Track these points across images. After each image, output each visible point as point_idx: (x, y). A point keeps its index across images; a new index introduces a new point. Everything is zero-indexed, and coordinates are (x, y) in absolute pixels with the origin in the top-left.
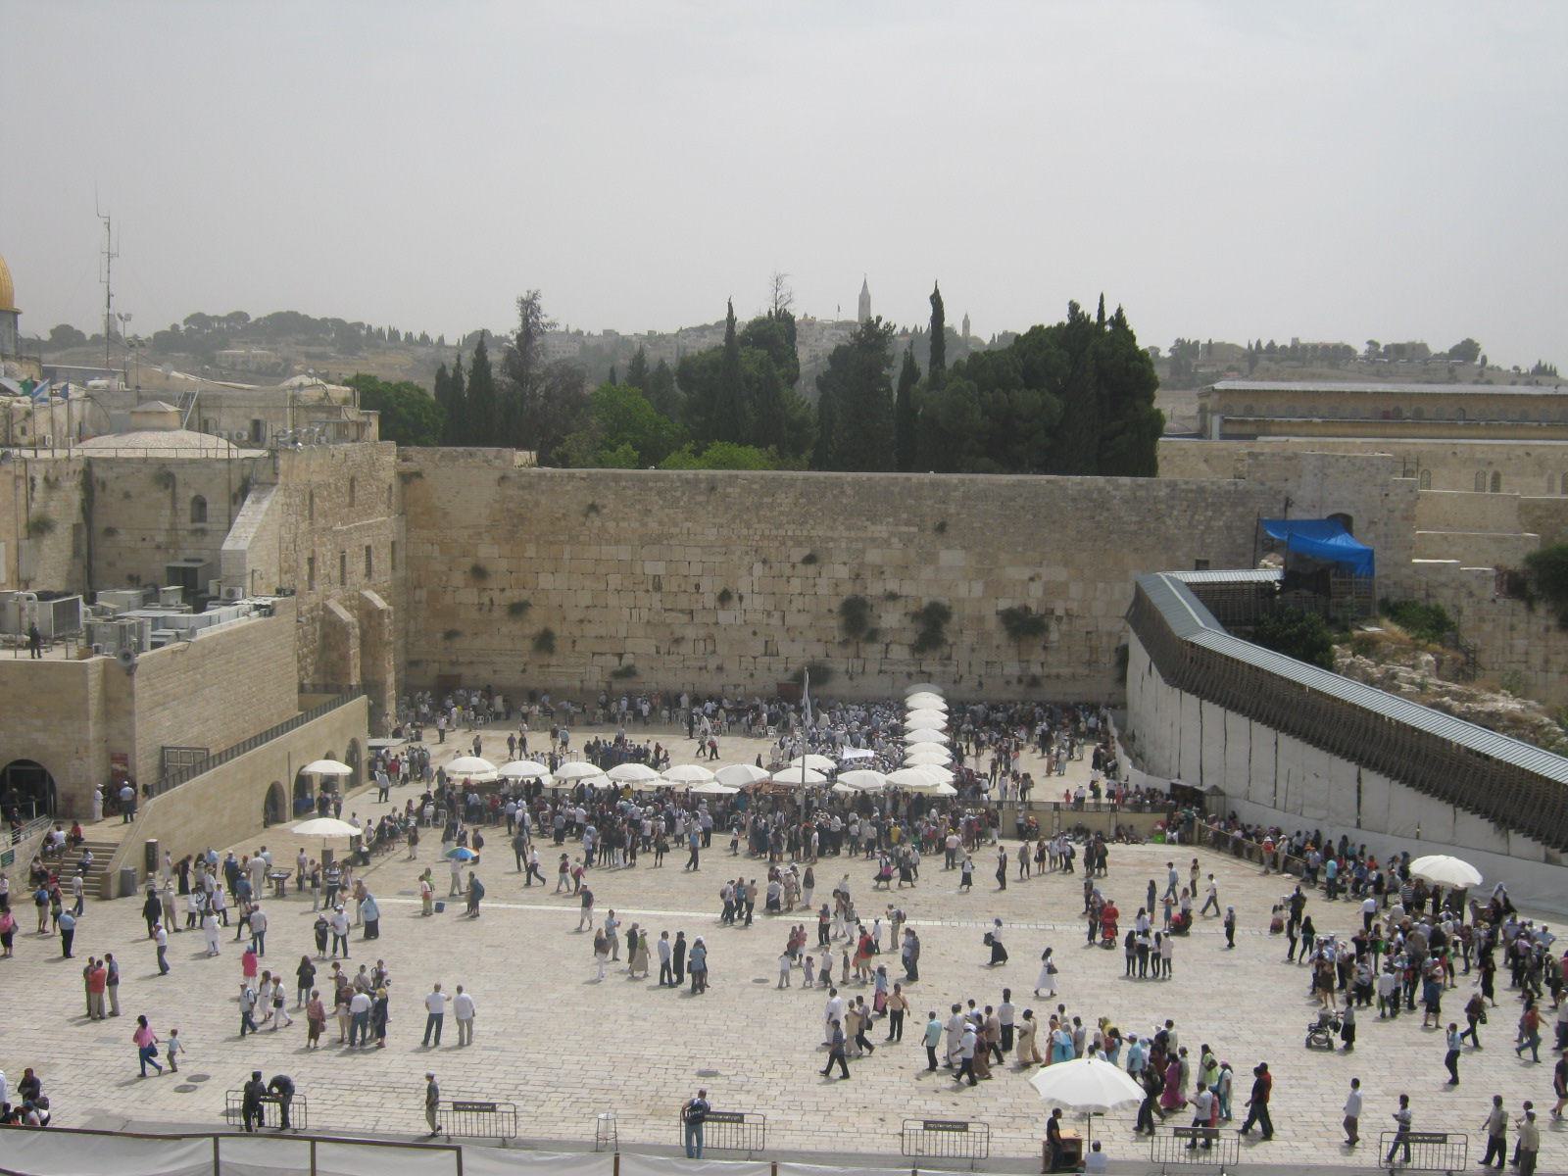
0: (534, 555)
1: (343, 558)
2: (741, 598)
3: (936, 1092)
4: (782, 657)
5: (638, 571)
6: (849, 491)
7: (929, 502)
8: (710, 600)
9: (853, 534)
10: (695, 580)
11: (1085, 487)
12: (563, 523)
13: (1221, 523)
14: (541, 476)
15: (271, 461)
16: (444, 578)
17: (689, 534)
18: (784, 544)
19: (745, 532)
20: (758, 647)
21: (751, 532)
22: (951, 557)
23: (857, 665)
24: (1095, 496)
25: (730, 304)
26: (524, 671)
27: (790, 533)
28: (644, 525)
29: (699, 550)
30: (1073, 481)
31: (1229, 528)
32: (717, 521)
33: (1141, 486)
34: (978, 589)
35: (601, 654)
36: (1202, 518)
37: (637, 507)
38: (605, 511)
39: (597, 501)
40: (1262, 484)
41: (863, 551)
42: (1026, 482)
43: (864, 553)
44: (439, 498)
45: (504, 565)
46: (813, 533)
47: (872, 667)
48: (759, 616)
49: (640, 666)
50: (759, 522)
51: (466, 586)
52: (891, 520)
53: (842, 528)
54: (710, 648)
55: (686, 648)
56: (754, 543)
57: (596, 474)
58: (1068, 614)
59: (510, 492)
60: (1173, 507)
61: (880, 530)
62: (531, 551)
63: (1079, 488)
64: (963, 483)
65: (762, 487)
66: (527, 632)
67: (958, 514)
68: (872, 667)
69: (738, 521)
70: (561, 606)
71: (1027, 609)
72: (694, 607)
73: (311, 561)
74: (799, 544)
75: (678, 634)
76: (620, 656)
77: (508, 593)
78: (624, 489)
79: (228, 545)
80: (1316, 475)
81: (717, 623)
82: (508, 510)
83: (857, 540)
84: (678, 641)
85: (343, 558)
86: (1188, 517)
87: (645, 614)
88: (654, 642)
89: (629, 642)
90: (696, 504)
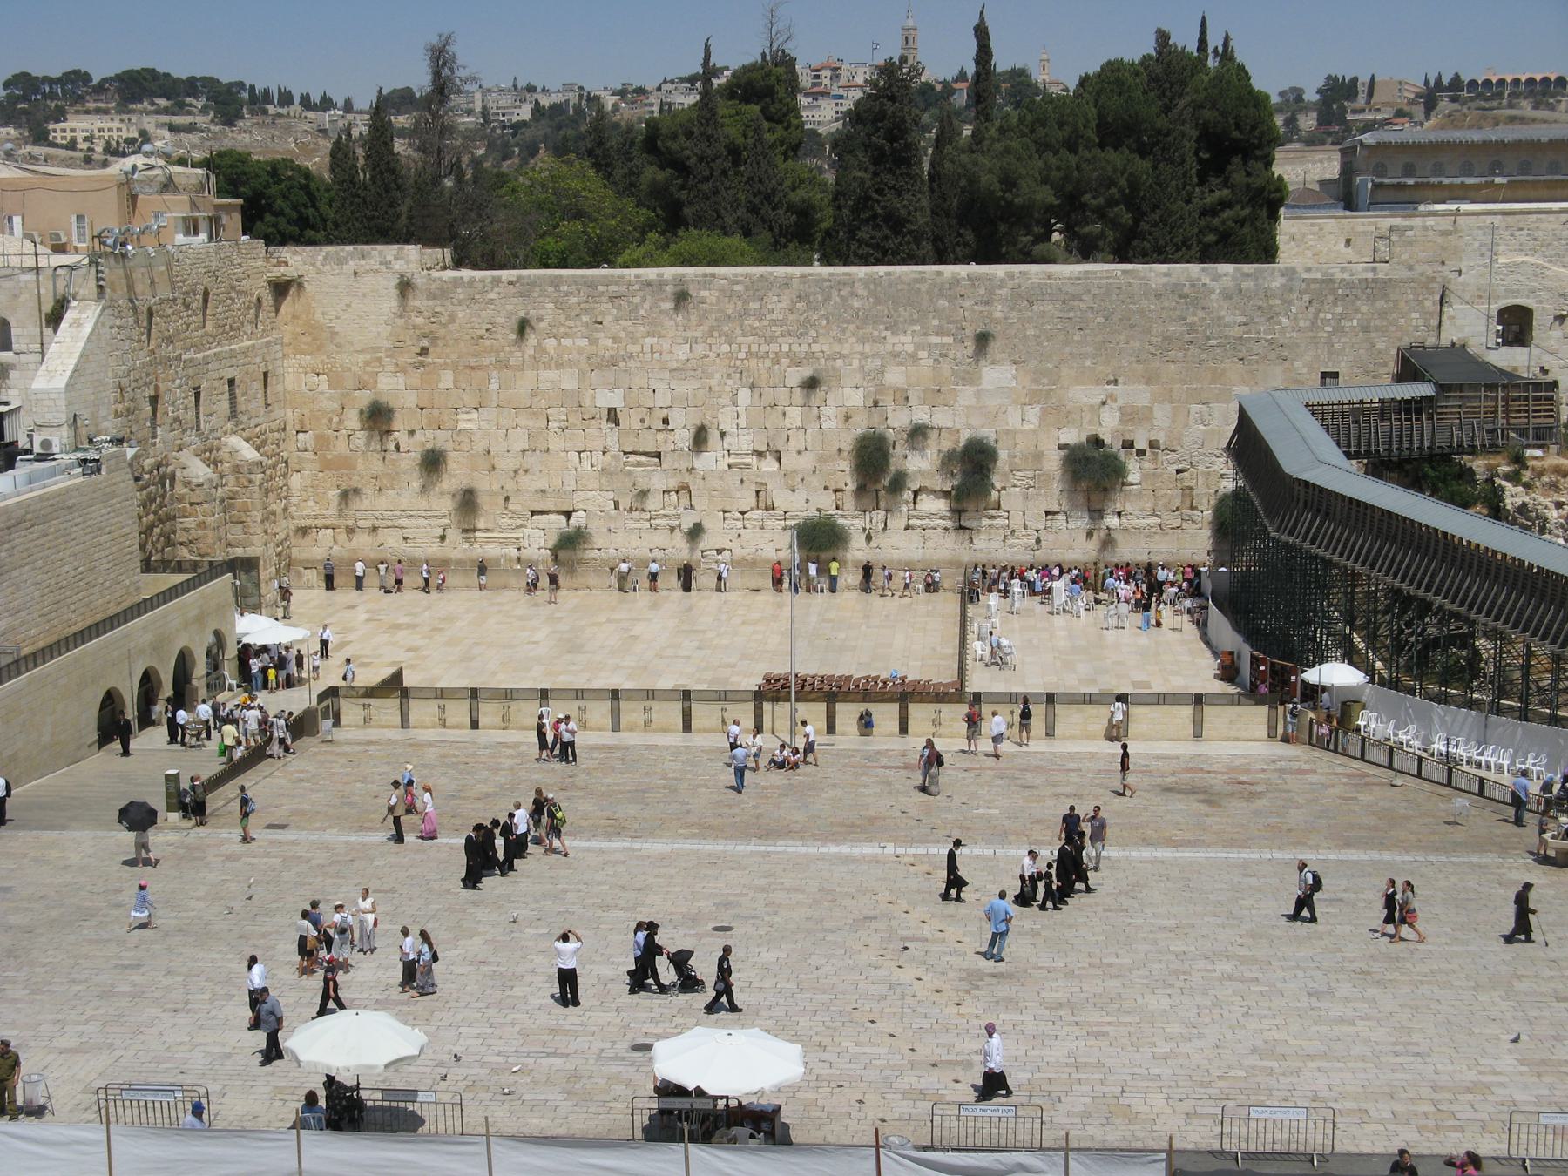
0: (451, 385)
1: (197, 396)
2: (723, 435)
3: (933, 1065)
4: (779, 512)
5: (587, 402)
6: (862, 291)
7: (967, 304)
8: (684, 438)
9: (867, 348)
11: (1173, 280)
12: (488, 342)
13: (1355, 323)
14: (457, 282)
15: (93, 270)
19: (726, 348)
21: (735, 347)
22: (997, 375)
24: (1187, 290)
25: (707, 47)
26: (443, 538)
27: (785, 348)
28: (593, 342)
29: (667, 375)
30: (1157, 273)
31: (1366, 329)
32: (689, 334)
33: (1248, 275)
34: (1033, 413)
36: (1329, 316)
37: (584, 318)
38: (542, 325)
39: (532, 312)
40: (1410, 268)
42: (1095, 273)
44: (324, 314)
45: (411, 400)
46: (816, 348)
52: (917, 328)
53: (853, 340)
55: (653, 503)
56: (739, 363)
57: (529, 276)
58: (1154, 445)
60: (1290, 303)
61: (905, 342)
62: (447, 379)
63: (1165, 280)
64: (1011, 276)
65: (747, 289)
67: (1006, 318)
69: (716, 334)
71: (1097, 442)
73: (154, 400)
75: (642, 485)
76: (568, 515)
77: (419, 436)
78: (566, 294)
79: (39, 383)
80: (1482, 255)
81: (691, 470)
82: (415, 327)
85: (197, 396)
86: (1311, 316)
88: (611, 495)
89: (578, 496)
90: (661, 312)
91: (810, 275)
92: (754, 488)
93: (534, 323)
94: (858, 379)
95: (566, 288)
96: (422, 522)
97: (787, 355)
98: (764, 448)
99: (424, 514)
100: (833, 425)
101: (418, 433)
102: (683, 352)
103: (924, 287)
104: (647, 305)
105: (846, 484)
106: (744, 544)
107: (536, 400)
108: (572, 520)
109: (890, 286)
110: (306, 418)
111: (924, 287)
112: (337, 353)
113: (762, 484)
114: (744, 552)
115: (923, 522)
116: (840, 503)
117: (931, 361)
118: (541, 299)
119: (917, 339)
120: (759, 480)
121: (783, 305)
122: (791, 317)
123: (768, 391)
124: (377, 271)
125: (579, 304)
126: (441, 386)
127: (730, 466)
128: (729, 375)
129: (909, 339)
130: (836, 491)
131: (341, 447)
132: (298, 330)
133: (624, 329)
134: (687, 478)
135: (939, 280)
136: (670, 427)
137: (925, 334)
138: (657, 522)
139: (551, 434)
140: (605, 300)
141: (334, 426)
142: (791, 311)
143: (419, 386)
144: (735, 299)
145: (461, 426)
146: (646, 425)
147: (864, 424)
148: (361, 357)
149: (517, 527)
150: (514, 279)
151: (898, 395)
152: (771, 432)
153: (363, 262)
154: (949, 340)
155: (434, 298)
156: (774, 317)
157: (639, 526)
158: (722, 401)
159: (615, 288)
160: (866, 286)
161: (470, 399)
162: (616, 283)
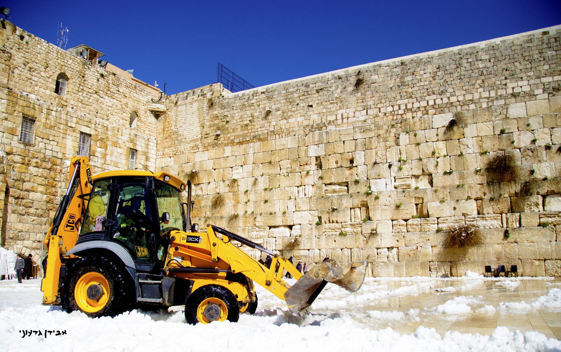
2: (390, 166)
5: (302, 154)
9: (493, 94)
10: (350, 156)
17: (343, 119)
19: (390, 109)
27: (431, 103)
35: (275, 227)
38: (279, 112)
41: (506, 106)
43: (507, 109)
46: (453, 99)
50: (401, 99)
53: (481, 90)
55: (344, 217)
56: (399, 117)
57: (273, 87)
59: (216, 112)
62: (228, 150)
69: (383, 101)
74: (440, 109)
76: (291, 227)
83: (497, 99)
88: (316, 213)
91: (445, 53)
92: (414, 201)
95: (292, 90)
97: (433, 107)
104: (339, 91)
105: (485, 194)
106: (407, 243)
107: (273, 157)
113: (419, 198)
115: (553, 220)
117: (546, 96)
120: (417, 195)
122: (434, 82)
123: (420, 133)
125: (299, 97)
127: (395, 188)
129: (525, 82)
136: (354, 165)
137: (539, 77)
144: (394, 77)
146: (339, 165)
150: (265, 90)
151: (521, 124)
156: (422, 84)
157: (334, 233)
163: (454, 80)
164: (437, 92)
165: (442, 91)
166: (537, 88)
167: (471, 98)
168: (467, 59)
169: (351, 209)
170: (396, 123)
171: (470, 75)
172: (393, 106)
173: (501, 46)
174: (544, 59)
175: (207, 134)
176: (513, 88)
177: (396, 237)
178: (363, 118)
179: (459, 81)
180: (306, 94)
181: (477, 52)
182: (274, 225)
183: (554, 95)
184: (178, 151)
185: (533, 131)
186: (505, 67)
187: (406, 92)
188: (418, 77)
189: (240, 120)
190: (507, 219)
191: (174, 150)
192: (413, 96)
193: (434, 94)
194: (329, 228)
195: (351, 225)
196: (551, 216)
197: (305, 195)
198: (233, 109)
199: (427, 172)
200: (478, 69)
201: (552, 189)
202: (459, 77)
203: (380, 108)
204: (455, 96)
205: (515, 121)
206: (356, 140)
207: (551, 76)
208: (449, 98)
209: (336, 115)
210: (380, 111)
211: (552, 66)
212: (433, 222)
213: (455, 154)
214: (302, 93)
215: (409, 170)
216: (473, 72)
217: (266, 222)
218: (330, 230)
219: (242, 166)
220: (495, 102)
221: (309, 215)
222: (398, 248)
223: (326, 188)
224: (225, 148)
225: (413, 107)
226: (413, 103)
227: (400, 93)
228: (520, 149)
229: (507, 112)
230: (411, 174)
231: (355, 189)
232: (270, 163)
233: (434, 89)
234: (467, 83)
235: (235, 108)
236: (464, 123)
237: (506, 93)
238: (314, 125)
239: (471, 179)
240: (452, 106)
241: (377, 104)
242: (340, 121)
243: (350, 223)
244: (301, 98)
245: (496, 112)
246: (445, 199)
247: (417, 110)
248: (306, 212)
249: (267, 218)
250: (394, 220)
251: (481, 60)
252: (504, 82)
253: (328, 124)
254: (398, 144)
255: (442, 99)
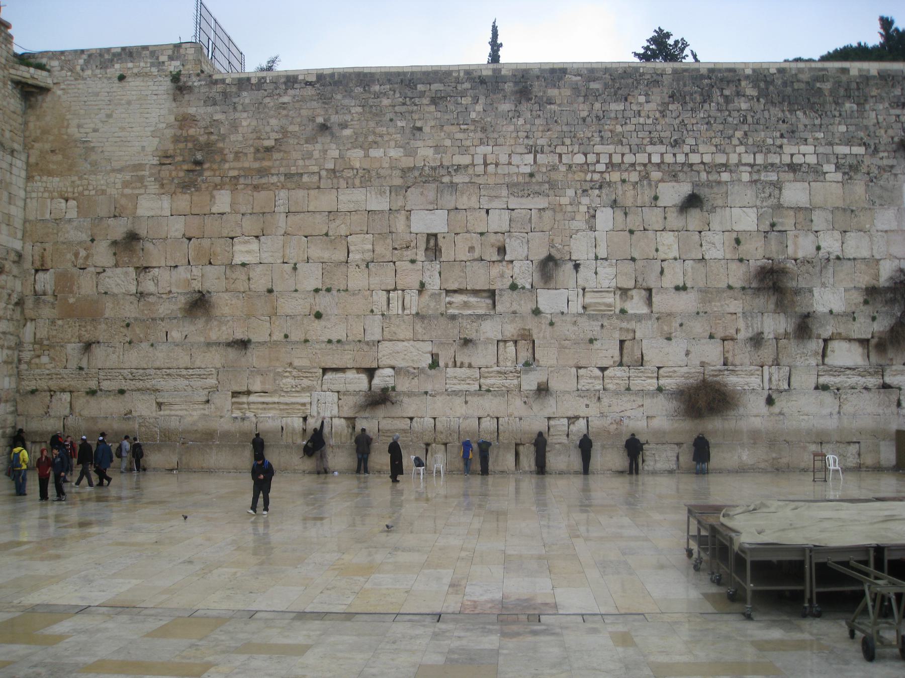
0: (228, 210)
2: (577, 267)
4: (650, 367)
8: (524, 273)
16: (83, 253)
17: (486, 164)
18: (647, 177)
19: (579, 159)
20: (608, 352)
21: (591, 158)
23: (778, 376)
27: (656, 159)
28: (411, 153)
37: (399, 124)
38: (347, 132)
39: (335, 118)
41: (778, 186)
43: (780, 189)
45: (177, 227)
46: (694, 158)
47: (805, 380)
48: (609, 299)
49: (404, 385)
51: (116, 265)
54: (524, 355)
55: (483, 356)
59: (192, 110)
61: (806, 154)
62: (223, 201)
65: (606, 86)
66: (214, 336)
68: (805, 380)
69: (568, 141)
70: (270, 291)
72: (497, 286)
76: (370, 372)
78: (377, 96)
81: (537, 312)
84: (467, 342)
87: (413, 301)
88: (428, 347)
89: (385, 348)
92: (617, 336)
93: (336, 129)
94: (749, 195)
96: (181, 383)
98: (631, 284)
99: (184, 372)
100: (719, 254)
101: (181, 269)
102: (524, 163)
103: (827, 86)
104: (479, 108)
107: (333, 225)
108: (376, 381)
109: (785, 84)
110: (47, 254)
111: (827, 86)
112: (94, 173)
113: (628, 330)
114: (606, 422)
115: (837, 380)
116: (730, 356)
117: (839, 176)
118: (346, 102)
119: (821, 150)
121: (652, 106)
124: (147, 75)
126: (215, 209)
127: (584, 308)
128: (584, 191)
129: (810, 149)
130: (724, 340)
131: (86, 285)
132: (47, 147)
133: (449, 136)
134: (531, 324)
135: (844, 78)
136: (507, 258)
137: (831, 144)
138: (489, 381)
139: (352, 269)
140: (426, 101)
141: (80, 261)
142: (663, 114)
143: (187, 211)
145: (238, 260)
146: (476, 255)
147: (760, 254)
148: (119, 178)
149: (304, 390)
150: (314, 79)
152: (640, 263)
153: (130, 65)
154: (861, 150)
155: (214, 105)
156: (642, 120)
157: (464, 387)
158: (575, 225)
159: (436, 86)
160: (756, 86)
161: (250, 225)
162: (441, 82)
163: (697, 123)
164: (668, 140)
165: (675, 141)
166: (828, 162)
167: (724, 161)
168: (722, 89)
169: (498, 341)
170: (592, 188)
171: (725, 120)
172: (585, 155)
173: (778, 79)
174: (840, 115)
175: (167, 157)
176: (792, 155)
177: (585, 399)
178: (528, 170)
179: (705, 126)
180: (408, 103)
181: (739, 80)
182: (334, 366)
183: (850, 178)
184: (91, 188)
185: (816, 232)
186: (780, 115)
187: (611, 131)
188: (634, 107)
189: (254, 136)
190: (771, 374)
191: (78, 182)
192: (624, 140)
193: (662, 143)
194: (455, 377)
195: (499, 372)
196: (835, 373)
197: (404, 308)
198: (235, 108)
199: (644, 284)
200: (738, 111)
201: (839, 331)
202: (707, 120)
203: (560, 155)
204: (698, 152)
205: (792, 213)
206: (513, 210)
207: (848, 145)
208: (687, 154)
209: (473, 155)
210: (560, 161)
211: (852, 128)
212: (649, 375)
213: (694, 257)
214: (401, 100)
215: (612, 278)
216: (730, 115)
217: (317, 360)
218: (455, 381)
219: (257, 237)
220: (763, 174)
221: (412, 349)
222: (587, 418)
223: (448, 299)
224: (215, 192)
225: (623, 162)
226: (623, 155)
227: (600, 132)
228: (796, 260)
229: (780, 193)
230: (613, 284)
231: (508, 305)
232: (327, 235)
233: (662, 134)
234: (719, 134)
235: (240, 107)
236: (710, 204)
237: (781, 162)
238: (426, 168)
239: (718, 304)
240: (692, 170)
241: (556, 146)
242: (480, 169)
243: (496, 368)
244: (397, 109)
245: (764, 192)
246: (673, 335)
247: (630, 169)
248: (405, 343)
249: (318, 352)
250: (580, 368)
251: (744, 96)
252: (778, 142)
253: (455, 170)
254: (593, 229)
255: (674, 155)
